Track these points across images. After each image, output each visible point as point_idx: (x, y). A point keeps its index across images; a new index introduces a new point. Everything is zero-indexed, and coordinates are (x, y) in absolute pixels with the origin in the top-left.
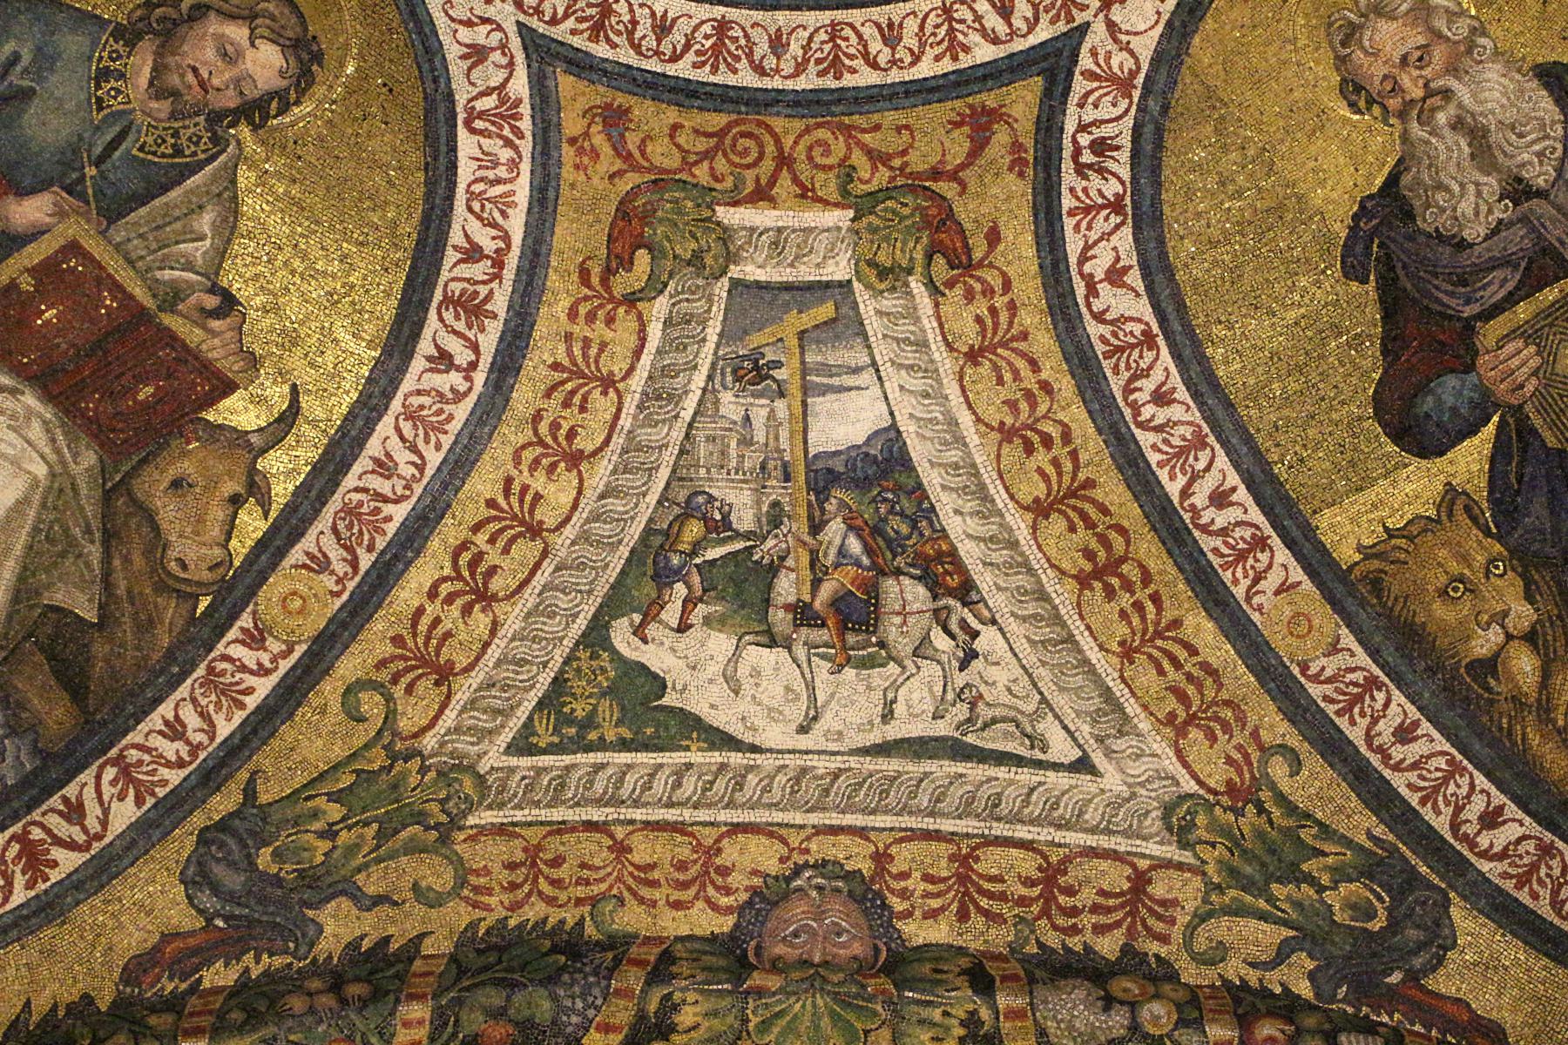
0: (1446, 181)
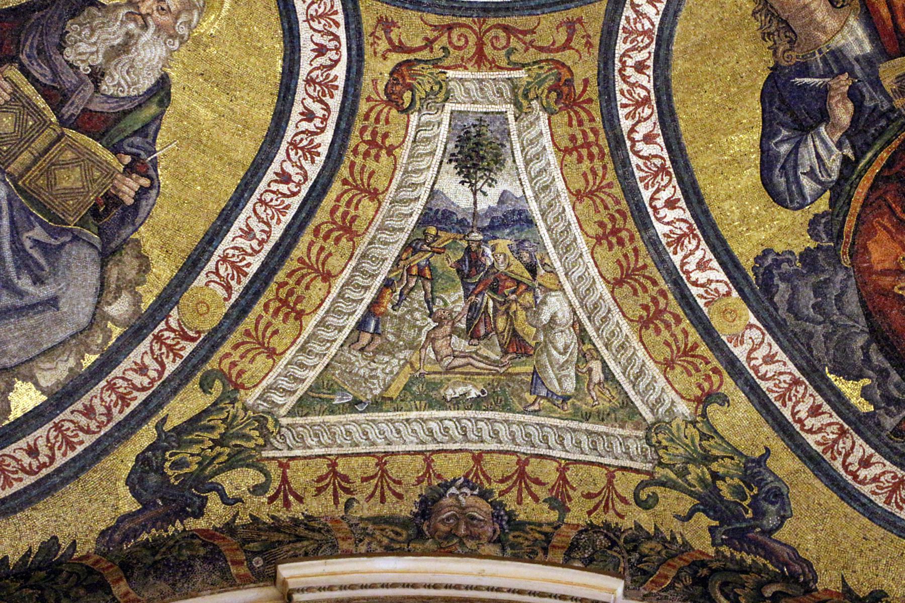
0: (96, 34)
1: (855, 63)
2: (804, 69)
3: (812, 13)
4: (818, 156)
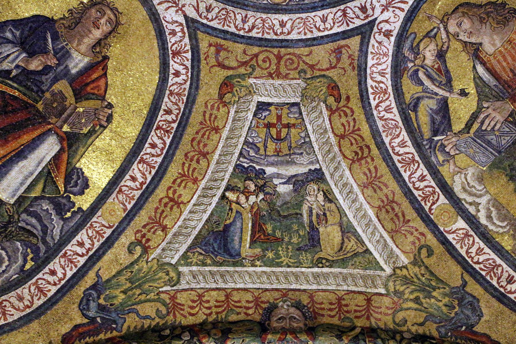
1: (64, 66)
2: (55, 38)
3: (87, 36)
4: (8, 55)
